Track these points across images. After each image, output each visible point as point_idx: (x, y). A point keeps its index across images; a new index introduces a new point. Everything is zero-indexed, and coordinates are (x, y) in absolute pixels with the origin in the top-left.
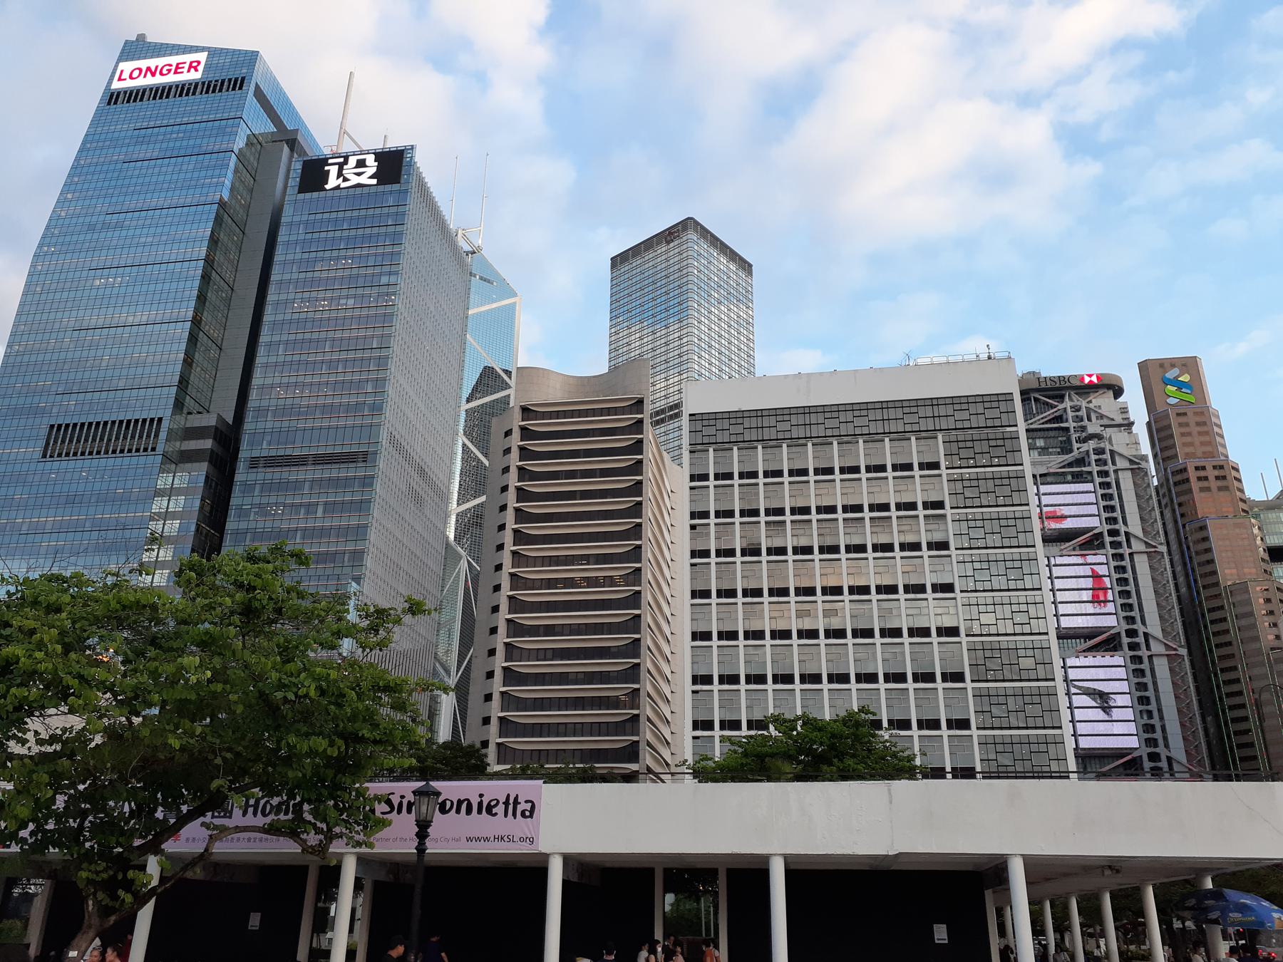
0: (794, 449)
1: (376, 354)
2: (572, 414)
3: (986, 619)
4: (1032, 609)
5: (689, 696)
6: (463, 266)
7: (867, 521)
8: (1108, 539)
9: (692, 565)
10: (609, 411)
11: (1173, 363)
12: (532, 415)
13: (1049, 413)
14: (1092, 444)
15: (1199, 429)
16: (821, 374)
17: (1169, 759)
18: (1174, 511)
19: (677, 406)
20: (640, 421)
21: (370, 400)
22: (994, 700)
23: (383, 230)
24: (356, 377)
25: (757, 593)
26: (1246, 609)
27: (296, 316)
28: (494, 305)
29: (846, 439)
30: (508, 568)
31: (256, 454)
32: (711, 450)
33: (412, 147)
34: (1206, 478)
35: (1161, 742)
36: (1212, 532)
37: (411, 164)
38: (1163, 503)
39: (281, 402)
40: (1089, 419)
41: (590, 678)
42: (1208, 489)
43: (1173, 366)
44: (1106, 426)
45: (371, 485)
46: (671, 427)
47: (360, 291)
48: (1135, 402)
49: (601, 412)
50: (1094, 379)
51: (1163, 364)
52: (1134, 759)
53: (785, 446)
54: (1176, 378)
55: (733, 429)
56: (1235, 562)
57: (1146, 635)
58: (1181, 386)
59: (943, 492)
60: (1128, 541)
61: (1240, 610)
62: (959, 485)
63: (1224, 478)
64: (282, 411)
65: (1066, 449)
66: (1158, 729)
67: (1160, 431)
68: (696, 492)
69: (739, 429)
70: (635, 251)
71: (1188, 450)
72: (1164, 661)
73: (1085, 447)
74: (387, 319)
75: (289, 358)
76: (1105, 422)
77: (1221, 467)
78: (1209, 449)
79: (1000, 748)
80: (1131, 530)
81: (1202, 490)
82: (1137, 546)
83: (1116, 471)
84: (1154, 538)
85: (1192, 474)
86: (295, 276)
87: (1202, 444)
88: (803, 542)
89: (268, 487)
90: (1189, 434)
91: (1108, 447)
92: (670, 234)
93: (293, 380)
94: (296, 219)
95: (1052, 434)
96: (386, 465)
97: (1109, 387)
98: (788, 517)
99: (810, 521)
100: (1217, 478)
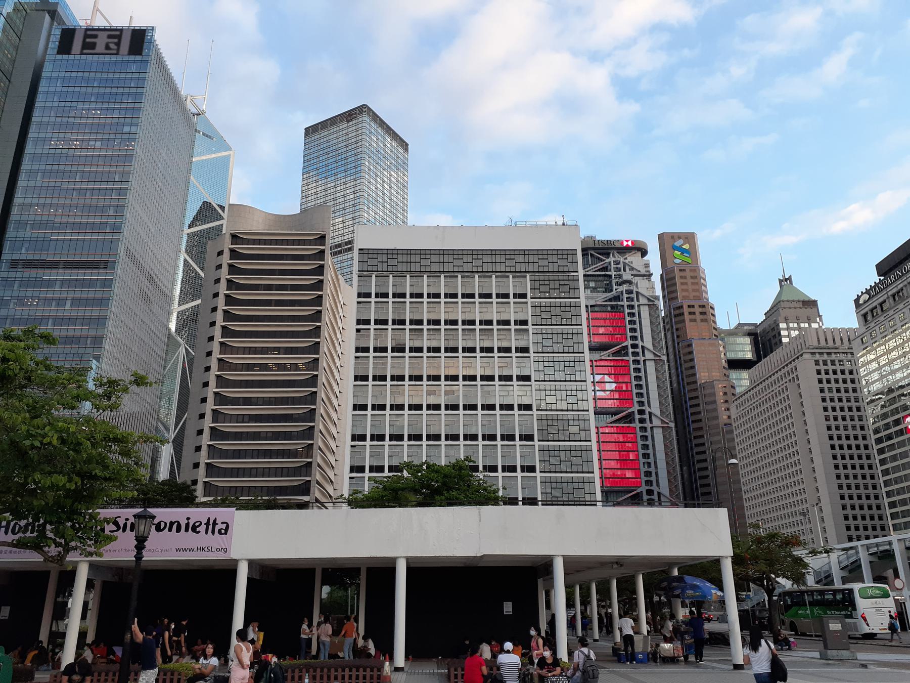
0: (432, 279)
1: (118, 186)
2: (270, 242)
3: (550, 399)
4: (579, 394)
5: (348, 449)
6: (190, 123)
7: (478, 331)
8: (630, 350)
9: (356, 357)
10: (299, 242)
11: (679, 236)
12: (238, 240)
13: (600, 265)
14: (625, 287)
15: (692, 281)
16: (453, 227)
17: (659, 494)
18: (673, 333)
19: (351, 242)
20: (323, 252)
21: (111, 221)
22: (552, 453)
23: (127, 90)
24: (101, 203)
25: (401, 378)
26: (712, 399)
27: (52, 151)
28: (213, 156)
29: (467, 274)
30: (216, 354)
31: (15, 257)
32: (374, 276)
33: (153, 28)
34: (694, 313)
35: (655, 483)
36: (695, 348)
37: (152, 41)
38: (667, 328)
39: (38, 218)
40: (625, 270)
41: (277, 436)
42: (695, 320)
43: (680, 238)
44: (635, 275)
45: (110, 286)
46: (346, 257)
47: (106, 136)
48: (654, 260)
49: (293, 242)
50: (630, 243)
51: (674, 236)
52: (638, 494)
53: (425, 276)
54: (681, 246)
55: (390, 262)
56: (707, 369)
57: (650, 413)
58: (683, 251)
59: (528, 314)
61: (708, 399)
62: (538, 309)
63: (705, 313)
64: (39, 225)
65: (608, 289)
66: (654, 474)
67: (668, 281)
68: (361, 305)
69: (394, 262)
71: (685, 294)
72: (660, 430)
73: (620, 289)
74: (128, 159)
75: (45, 184)
76: (635, 272)
77: (704, 306)
78: (697, 294)
79: (554, 485)
80: (645, 345)
81: (691, 320)
82: (649, 355)
84: (659, 351)
85: (686, 310)
86: (52, 120)
87: (694, 290)
88: (434, 344)
89: (25, 284)
90: (686, 284)
91: (635, 290)
92: (350, 115)
93: (48, 201)
94: (55, 74)
95: (600, 278)
96: (123, 271)
97: (639, 249)
98: (425, 327)
99: (440, 330)
100: (701, 313)
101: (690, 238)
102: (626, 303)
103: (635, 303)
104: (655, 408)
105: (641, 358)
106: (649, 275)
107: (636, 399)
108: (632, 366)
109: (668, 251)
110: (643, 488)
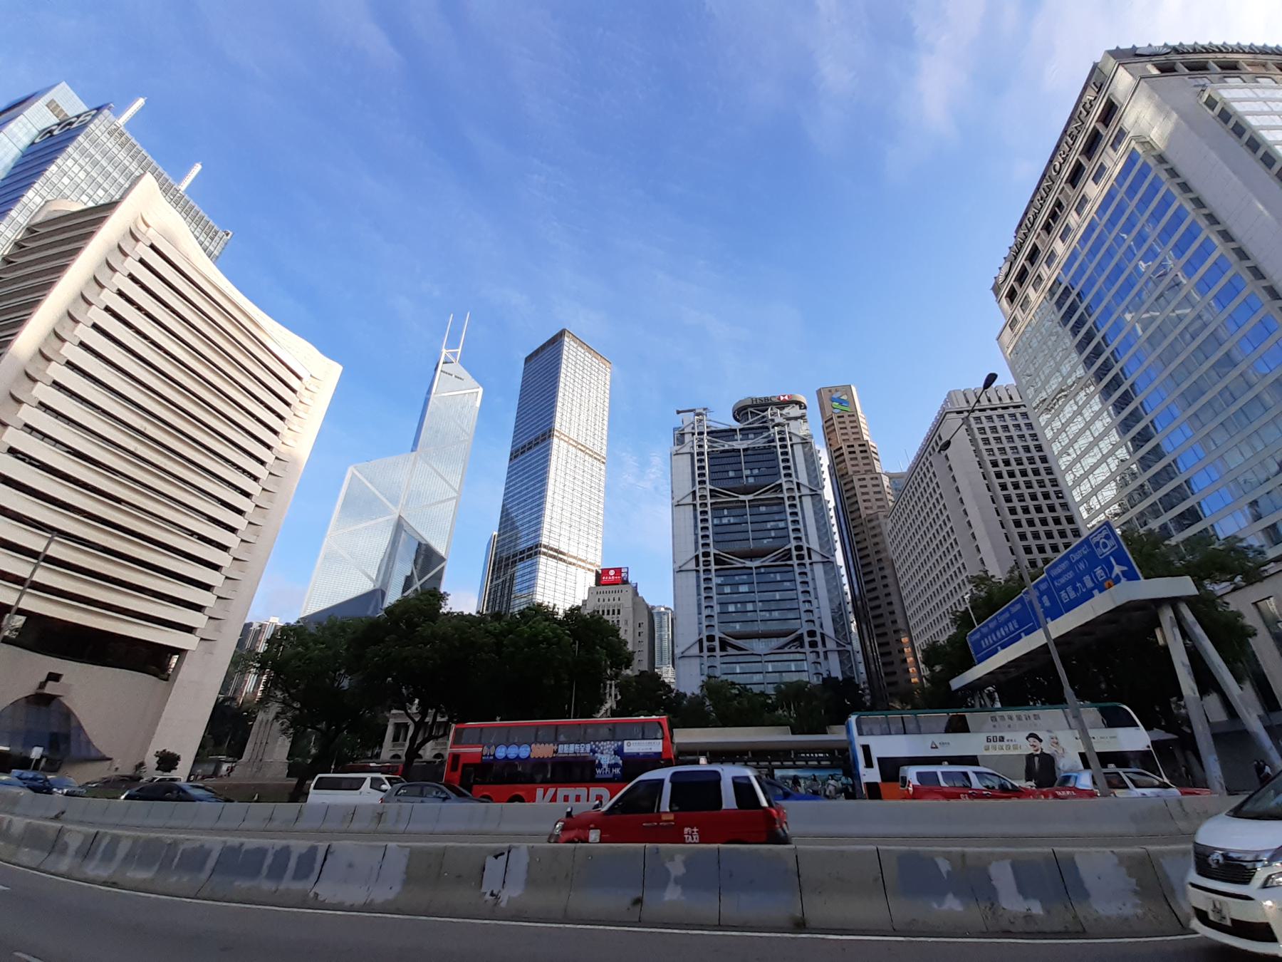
8: (785, 487)
17: (823, 635)
57: (809, 549)
58: (841, 402)
70: (536, 353)
72: (821, 566)
82: (805, 491)
85: (845, 450)
102: (778, 444)
103: (789, 443)
104: (815, 545)
105: (797, 494)
107: (792, 535)
108: (787, 503)
109: (827, 403)
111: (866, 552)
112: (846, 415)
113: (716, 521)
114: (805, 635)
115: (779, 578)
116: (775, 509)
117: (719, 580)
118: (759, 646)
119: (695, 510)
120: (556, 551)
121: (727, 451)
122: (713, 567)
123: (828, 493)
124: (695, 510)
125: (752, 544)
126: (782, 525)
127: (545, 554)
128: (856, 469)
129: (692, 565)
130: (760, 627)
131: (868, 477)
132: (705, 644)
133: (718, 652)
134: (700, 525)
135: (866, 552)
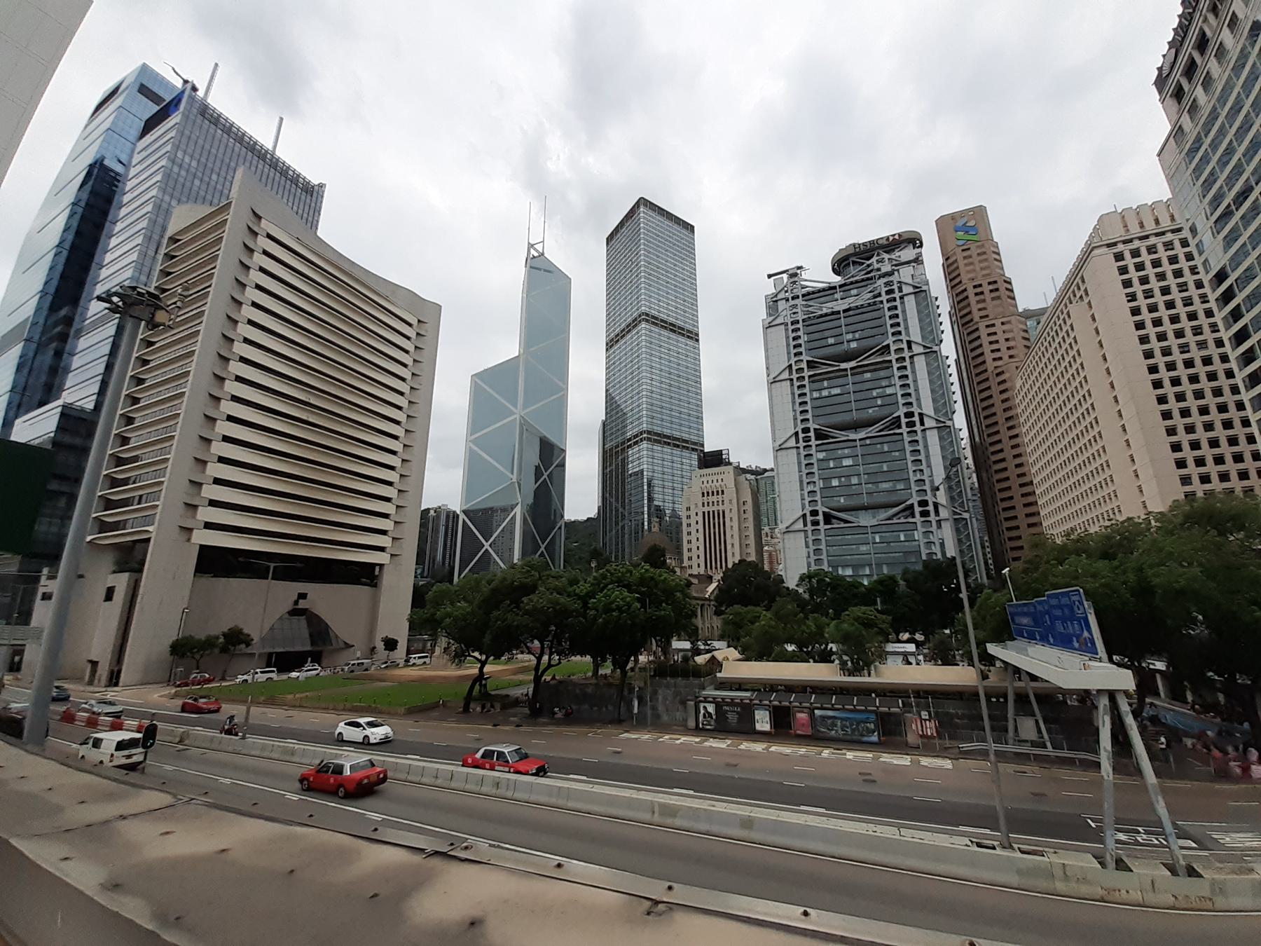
8: (893, 348)
11: (962, 214)
17: (936, 505)
42: (984, 301)
51: (953, 217)
57: (921, 415)
58: (966, 229)
60: (910, 347)
72: (935, 431)
77: (995, 282)
82: (917, 349)
83: (901, 298)
101: (979, 213)
102: (884, 298)
103: (897, 295)
104: (928, 409)
105: (906, 354)
106: (918, 260)
107: (901, 401)
108: (895, 365)
110: (914, 500)
111: (993, 410)
112: (973, 247)
113: (816, 395)
114: (916, 505)
115: (886, 449)
116: (882, 373)
117: (821, 455)
118: (866, 520)
119: (792, 385)
120: (659, 435)
121: (826, 315)
122: (813, 442)
123: (948, 348)
124: (792, 385)
125: (855, 415)
126: (889, 391)
127: (649, 439)
128: (983, 313)
129: (792, 443)
130: (865, 500)
131: (998, 322)
132: (809, 518)
133: (822, 526)
134: (798, 401)
135: (993, 410)
